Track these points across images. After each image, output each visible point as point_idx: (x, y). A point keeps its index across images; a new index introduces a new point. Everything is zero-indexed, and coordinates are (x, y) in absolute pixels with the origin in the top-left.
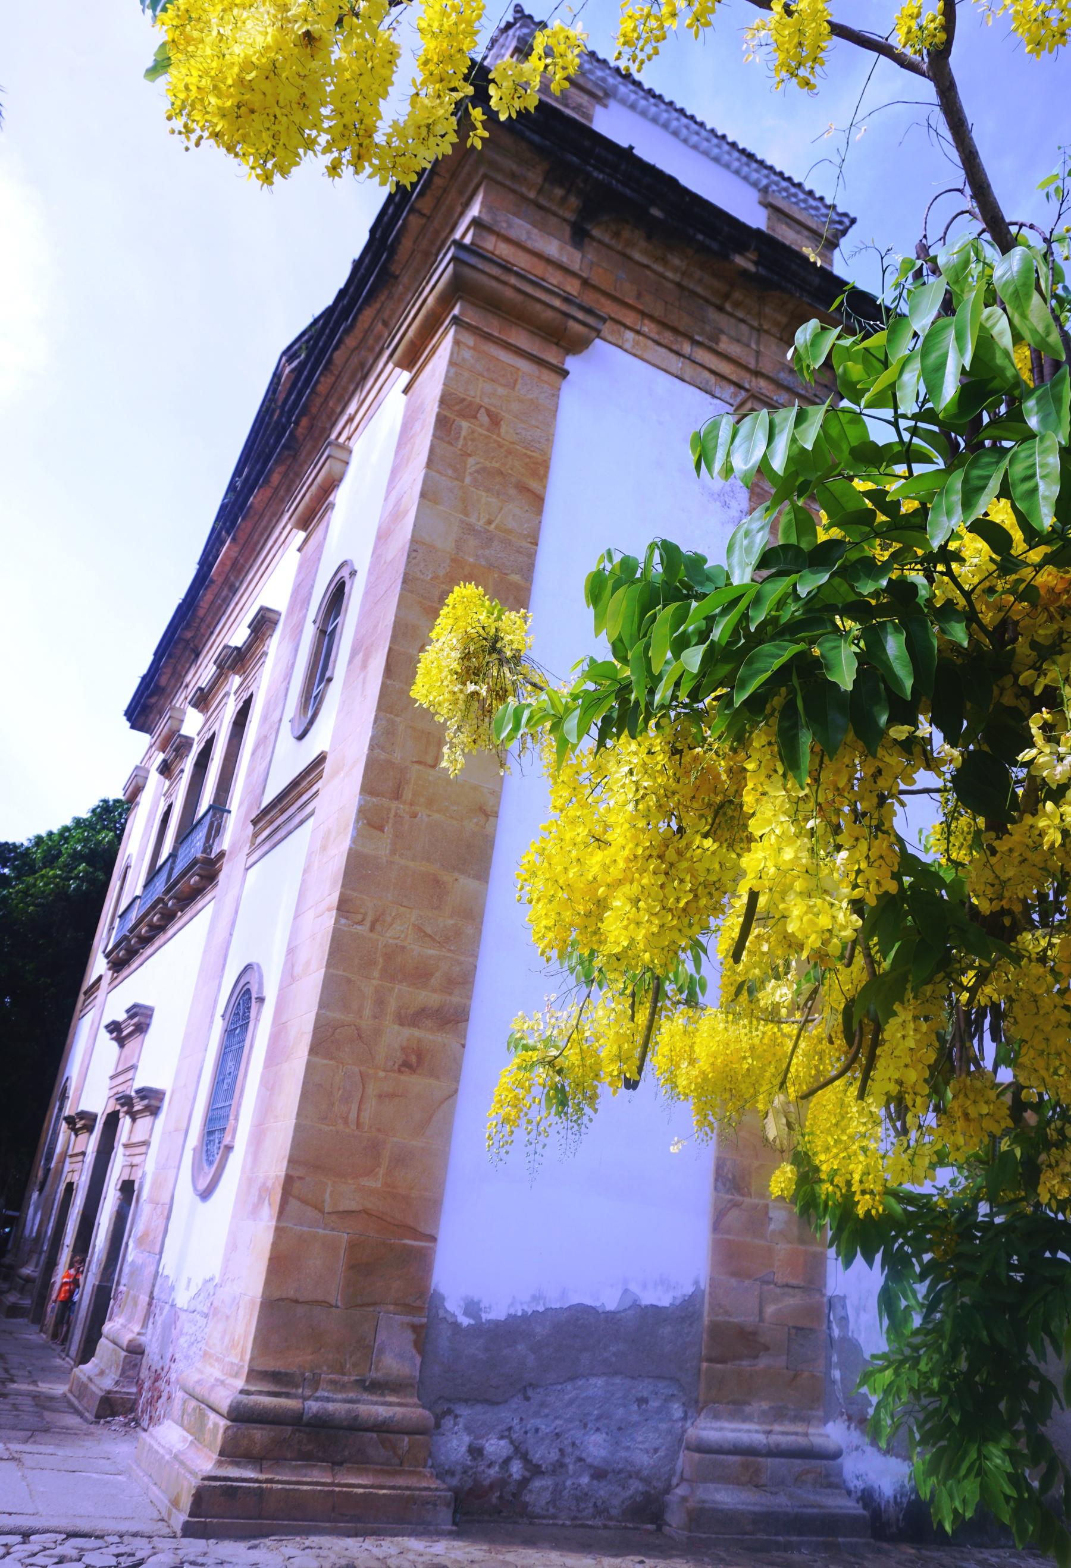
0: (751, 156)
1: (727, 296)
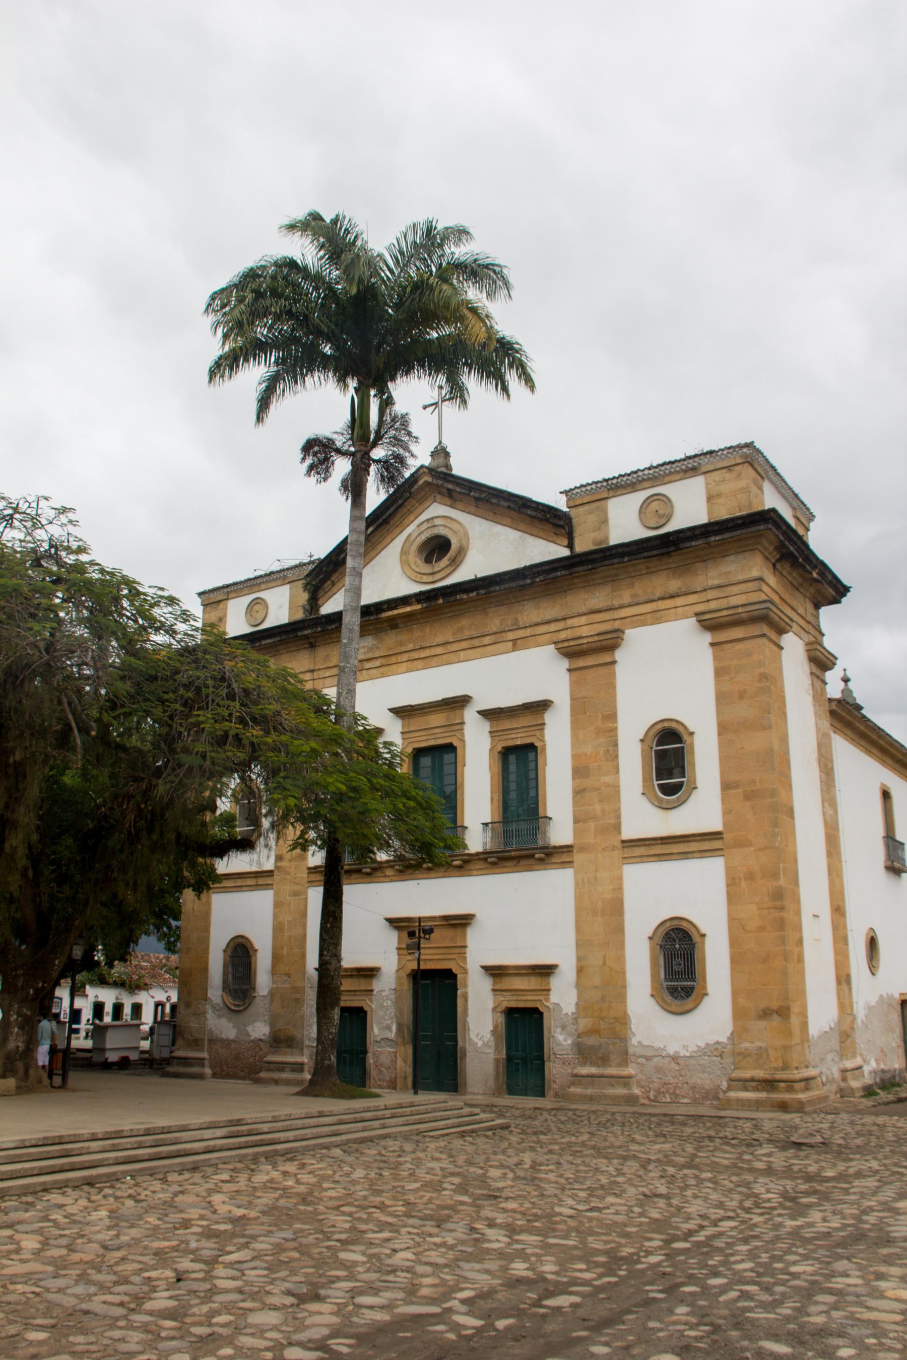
0: (796, 496)
1: (801, 585)
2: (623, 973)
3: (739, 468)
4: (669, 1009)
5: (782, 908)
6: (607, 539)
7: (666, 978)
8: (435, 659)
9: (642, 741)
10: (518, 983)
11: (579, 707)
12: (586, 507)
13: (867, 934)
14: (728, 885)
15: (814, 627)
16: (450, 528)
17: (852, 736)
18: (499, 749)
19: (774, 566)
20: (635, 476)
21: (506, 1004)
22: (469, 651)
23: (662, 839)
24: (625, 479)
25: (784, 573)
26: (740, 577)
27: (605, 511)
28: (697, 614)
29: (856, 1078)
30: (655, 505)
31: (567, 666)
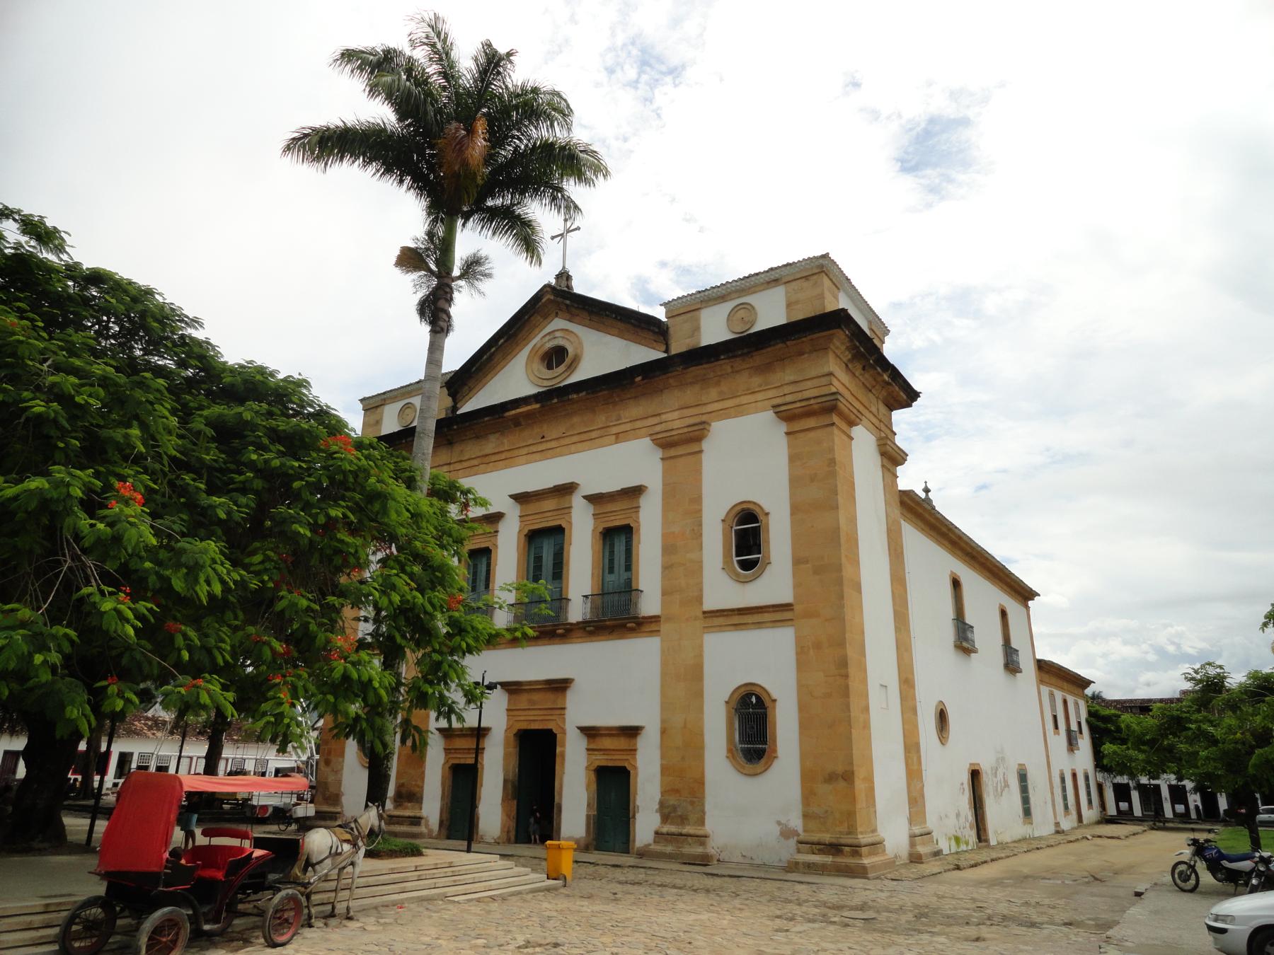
2: (702, 735)
3: (815, 277)
4: (744, 772)
5: (847, 676)
6: (699, 343)
7: (740, 741)
8: (550, 451)
9: (723, 521)
10: (607, 743)
11: (670, 492)
12: (683, 317)
13: (936, 707)
14: (797, 654)
15: (886, 426)
16: (568, 339)
17: (923, 526)
18: (601, 530)
19: (847, 366)
20: (724, 287)
21: (598, 763)
22: (579, 445)
23: (739, 610)
24: (715, 290)
25: (857, 374)
26: (813, 374)
27: (698, 320)
28: (774, 407)
29: (923, 844)
30: (742, 313)
31: (661, 456)
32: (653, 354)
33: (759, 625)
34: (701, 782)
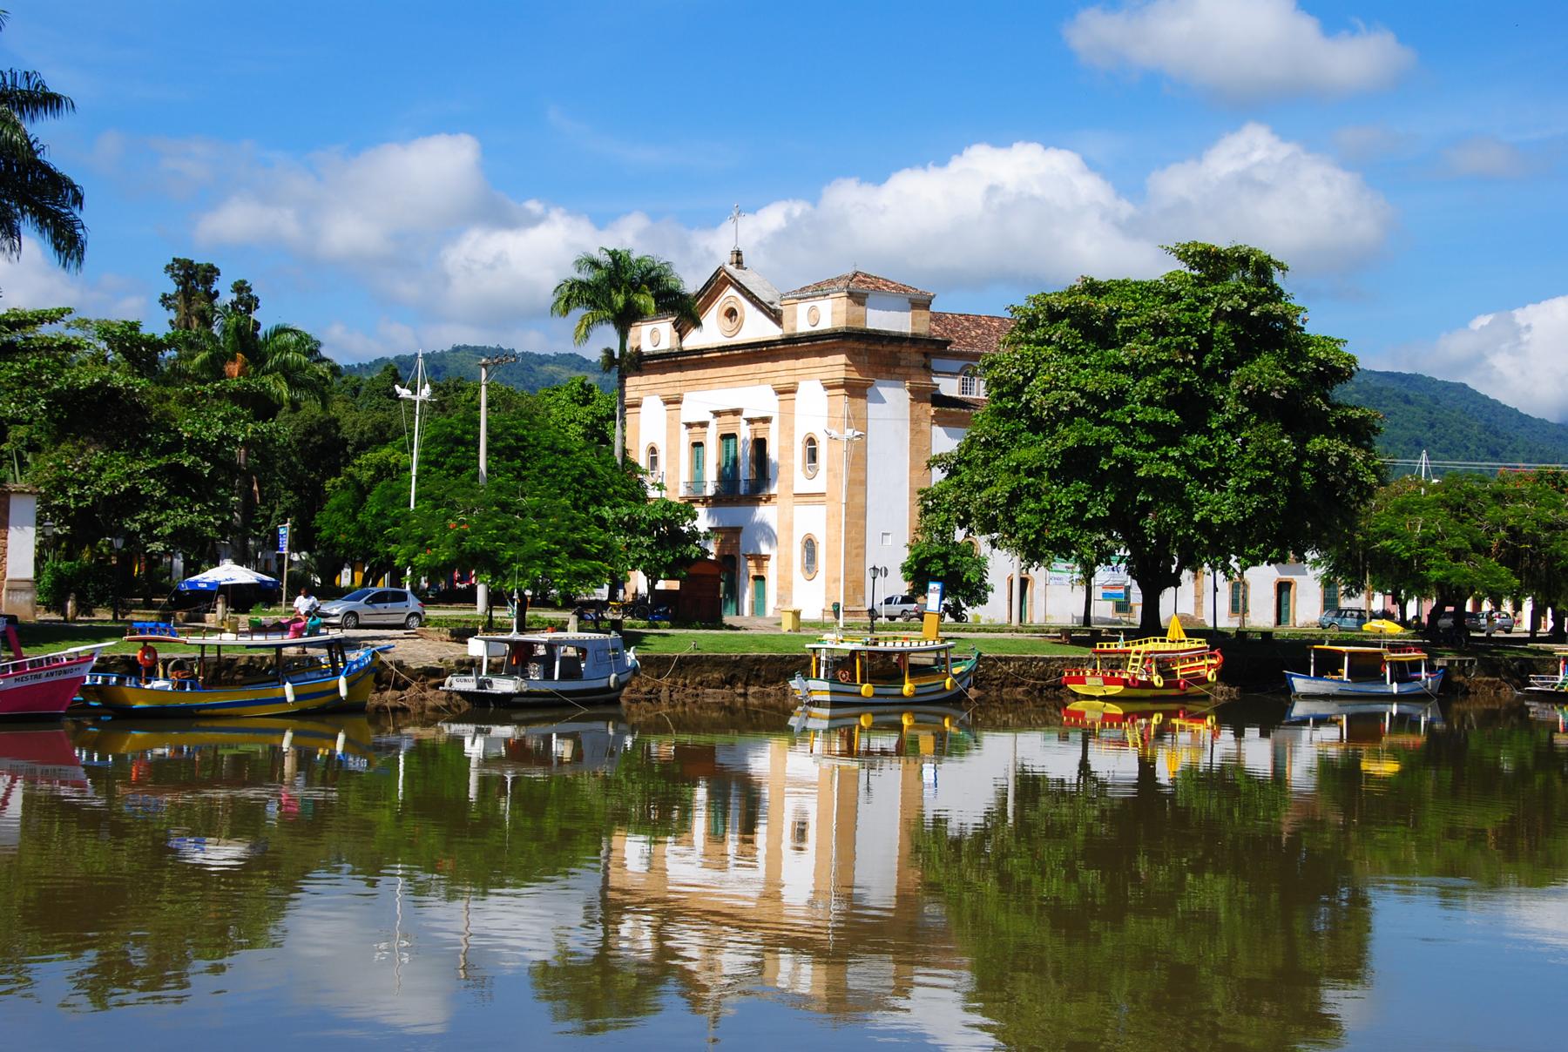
32: (770, 331)
33: (813, 503)
34: (791, 583)
